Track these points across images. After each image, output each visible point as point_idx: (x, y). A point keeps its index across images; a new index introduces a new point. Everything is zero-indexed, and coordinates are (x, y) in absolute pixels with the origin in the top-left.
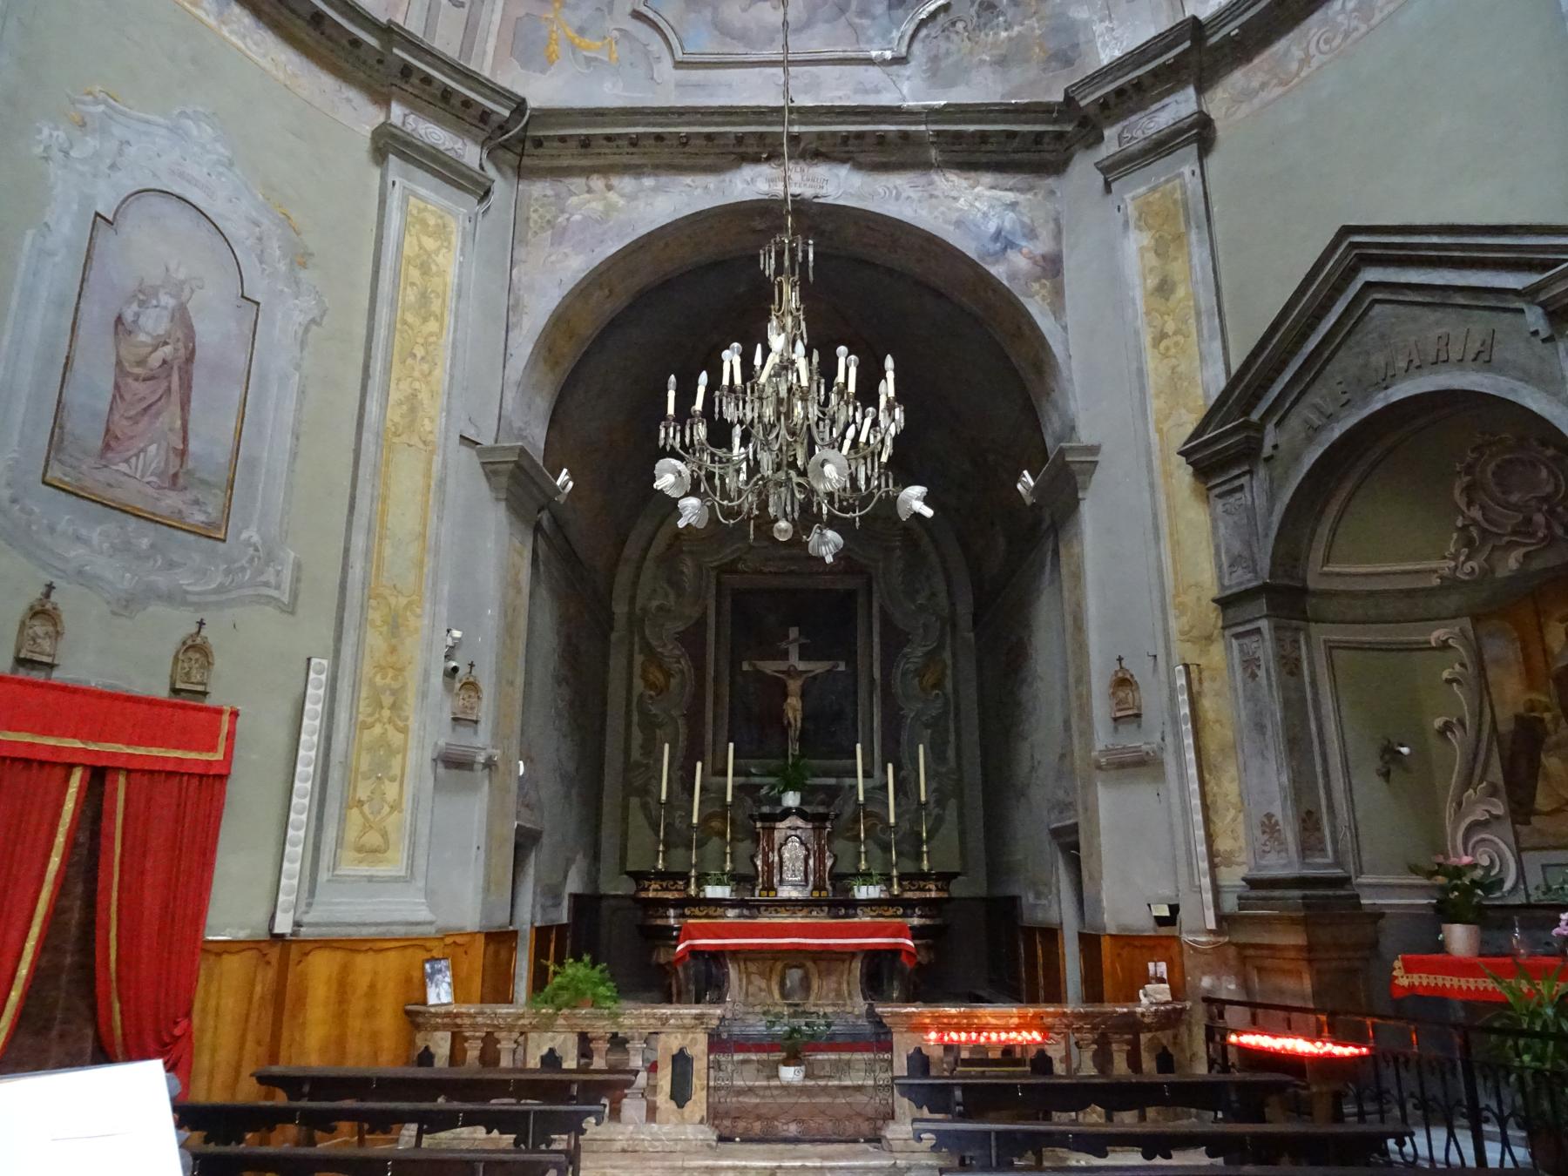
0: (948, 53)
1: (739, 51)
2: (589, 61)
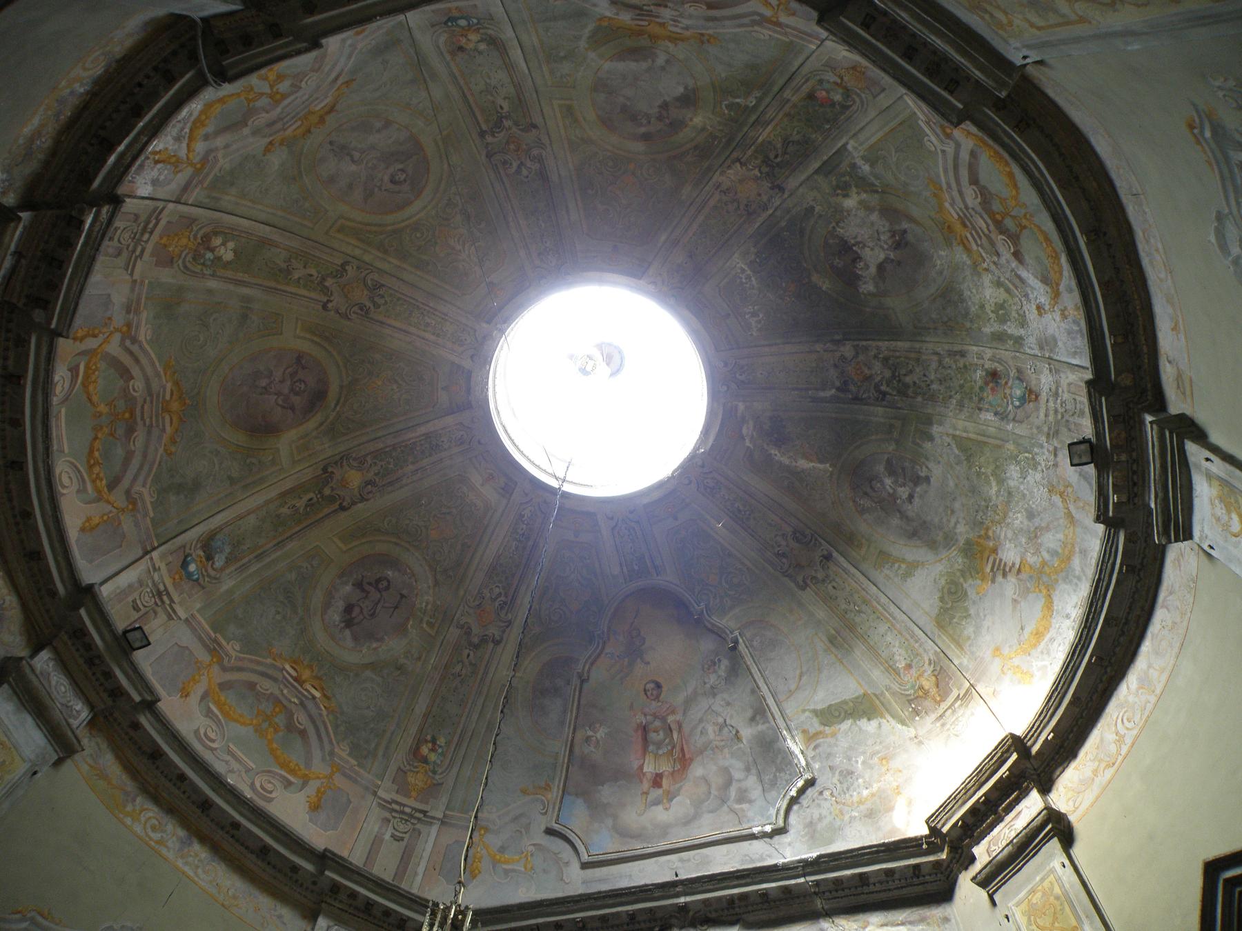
0: (820, 819)
1: (638, 847)
2: (506, 872)
